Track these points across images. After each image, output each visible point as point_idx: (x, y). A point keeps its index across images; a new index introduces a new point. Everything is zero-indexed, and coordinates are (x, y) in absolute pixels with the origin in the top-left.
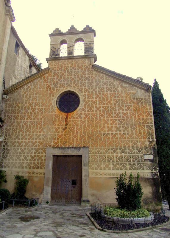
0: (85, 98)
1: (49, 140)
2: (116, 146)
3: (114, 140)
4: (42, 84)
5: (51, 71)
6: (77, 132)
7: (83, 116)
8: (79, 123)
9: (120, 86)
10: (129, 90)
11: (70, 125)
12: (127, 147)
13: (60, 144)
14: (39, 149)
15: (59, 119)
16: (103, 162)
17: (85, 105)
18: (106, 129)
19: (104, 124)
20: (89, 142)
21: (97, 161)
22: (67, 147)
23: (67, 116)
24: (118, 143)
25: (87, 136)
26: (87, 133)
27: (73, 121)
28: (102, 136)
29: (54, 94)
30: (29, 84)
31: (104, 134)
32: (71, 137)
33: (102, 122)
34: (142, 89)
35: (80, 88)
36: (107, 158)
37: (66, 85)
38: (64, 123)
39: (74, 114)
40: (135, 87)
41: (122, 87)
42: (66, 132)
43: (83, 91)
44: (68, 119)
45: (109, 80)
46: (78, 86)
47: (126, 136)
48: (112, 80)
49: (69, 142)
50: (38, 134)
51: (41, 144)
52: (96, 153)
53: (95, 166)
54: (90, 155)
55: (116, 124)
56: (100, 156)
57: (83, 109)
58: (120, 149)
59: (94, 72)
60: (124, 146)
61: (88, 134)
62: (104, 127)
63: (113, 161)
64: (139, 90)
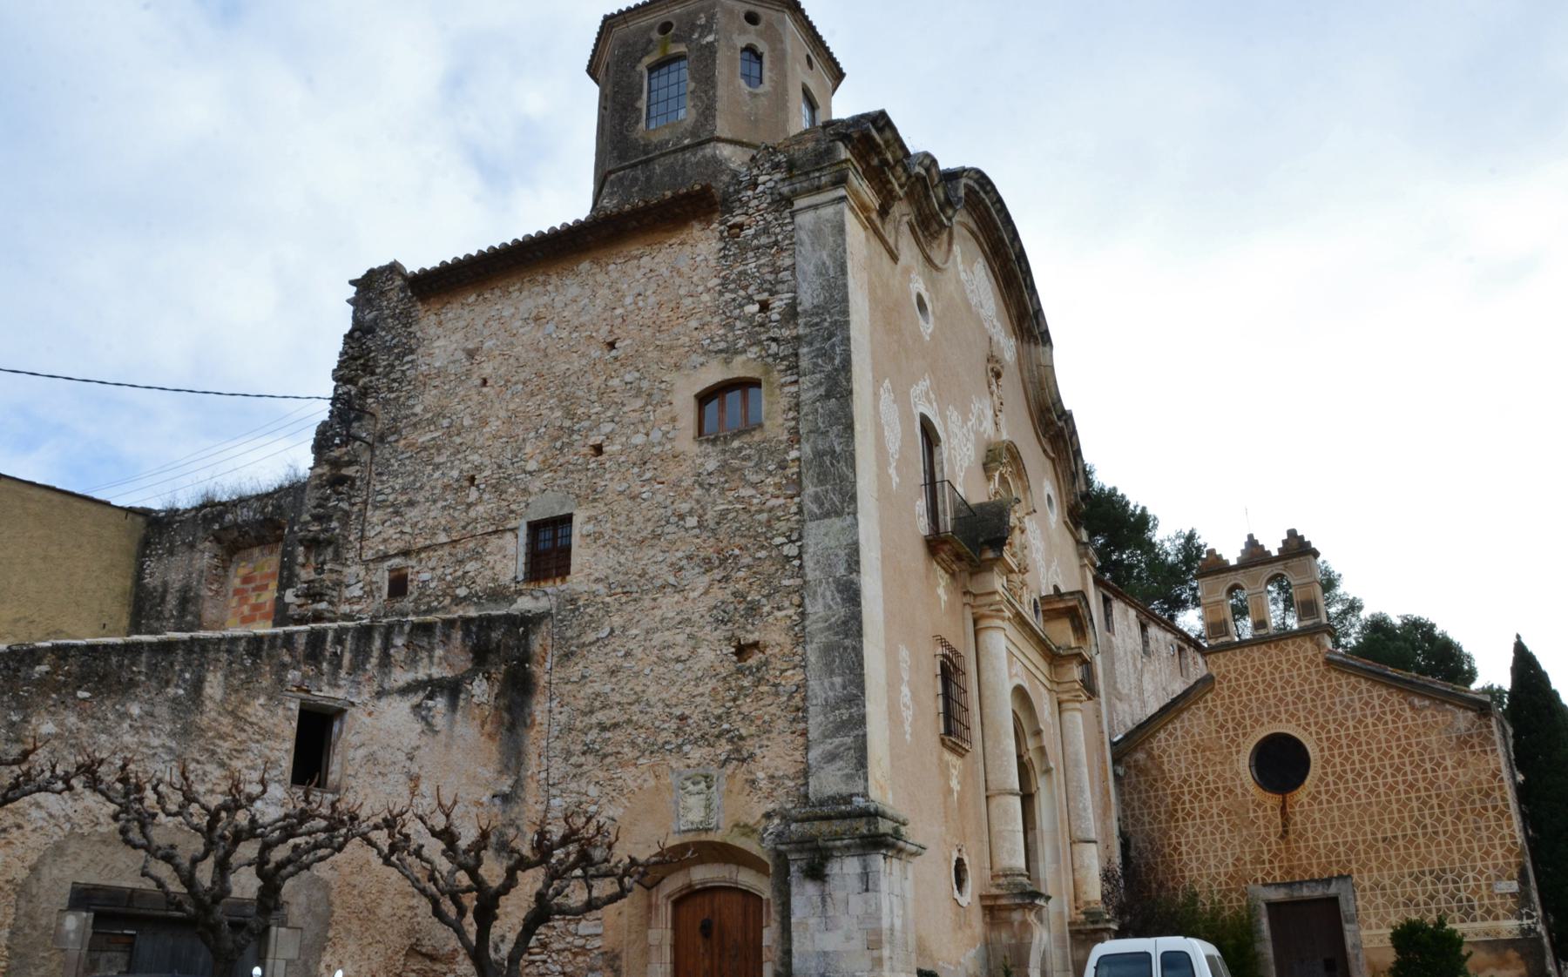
0: (1322, 750)
1: (1249, 867)
2: (1420, 865)
3: (1412, 851)
4: (1204, 721)
5: (1220, 683)
6: (1315, 839)
7: (1324, 797)
8: (1317, 816)
9: (1406, 706)
10: (1433, 716)
11: (1295, 824)
12: (1447, 866)
13: (1277, 873)
14: (1230, 890)
15: (1265, 810)
16: (1392, 910)
17: (1323, 767)
18: (1388, 826)
19: (1380, 814)
20: (1349, 861)
21: (1377, 908)
22: (1297, 879)
23: (1284, 802)
24: (1424, 859)
25: (1342, 849)
26: (1340, 840)
27: (1301, 813)
28: (1380, 845)
29: (1238, 745)
30: (1170, 726)
31: (1384, 840)
32: (1303, 853)
33: (1375, 809)
34: (1466, 708)
35: (1303, 722)
36: (1401, 899)
37: (1265, 719)
38: (1279, 820)
39: (1302, 795)
40: (1448, 706)
41: (1412, 707)
42: (1288, 843)
43: (1313, 729)
44: (1288, 810)
45: (1375, 694)
46: (1299, 719)
47: (1442, 838)
48: (1384, 692)
49: (1300, 866)
50: (1220, 853)
51: (1231, 878)
52: (1372, 889)
53: (1373, 921)
54: (1358, 894)
55: (1412, 810)
56: (1383, 895)
57: (1321, 780)
58: (1431, 872)
59: (1333, 675)
60: (1440, 863)
61: (1345, 843)
62: (1383, 821)
63: (1417, 905)
64: (1460, 713)
